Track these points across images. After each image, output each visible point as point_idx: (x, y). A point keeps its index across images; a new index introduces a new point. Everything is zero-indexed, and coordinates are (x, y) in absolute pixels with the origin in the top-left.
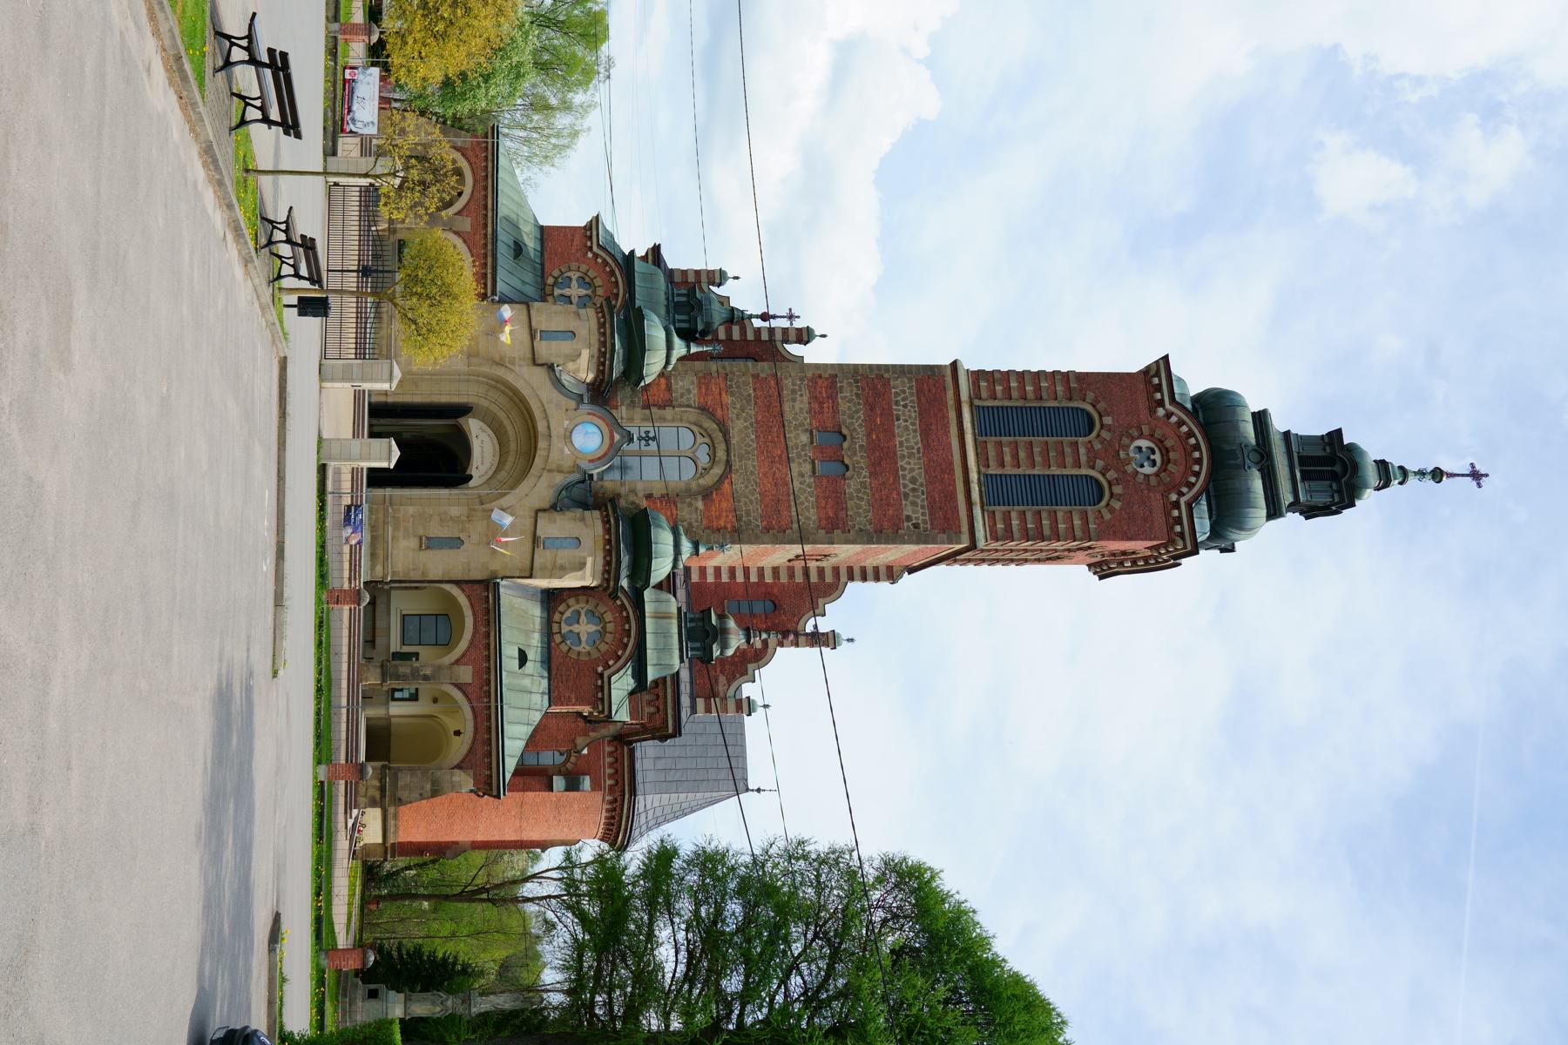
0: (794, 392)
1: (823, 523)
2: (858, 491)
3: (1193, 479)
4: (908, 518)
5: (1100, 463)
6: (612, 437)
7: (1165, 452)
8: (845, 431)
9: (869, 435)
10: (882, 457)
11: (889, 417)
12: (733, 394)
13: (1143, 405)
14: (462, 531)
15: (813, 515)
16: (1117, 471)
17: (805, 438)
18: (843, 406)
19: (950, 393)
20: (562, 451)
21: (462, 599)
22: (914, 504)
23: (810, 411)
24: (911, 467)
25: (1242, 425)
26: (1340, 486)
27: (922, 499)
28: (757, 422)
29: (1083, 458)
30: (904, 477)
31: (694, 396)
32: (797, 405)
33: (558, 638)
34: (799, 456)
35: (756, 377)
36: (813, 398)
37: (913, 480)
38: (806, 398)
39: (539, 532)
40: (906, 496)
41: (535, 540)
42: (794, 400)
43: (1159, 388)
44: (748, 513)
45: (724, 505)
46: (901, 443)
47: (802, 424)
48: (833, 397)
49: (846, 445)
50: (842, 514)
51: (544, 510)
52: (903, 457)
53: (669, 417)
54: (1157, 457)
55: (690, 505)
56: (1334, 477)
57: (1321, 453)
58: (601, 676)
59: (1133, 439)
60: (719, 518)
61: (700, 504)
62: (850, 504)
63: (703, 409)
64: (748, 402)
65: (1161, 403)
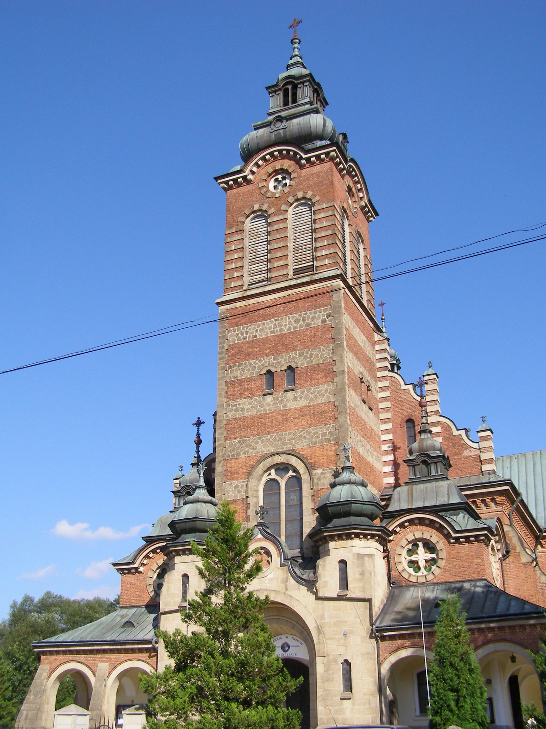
0: (237, 410)
1: (328, 379)
2: (305, 357)
3: (292, 153)
4: (323, 321)
5: (284, 207)
6: (260, 540)
7: (276, 172)
8: (264, 371)
9: (267, 355)
10: (281, 344)
11: (255, 342)
12: (238, 454)
13: (246, 188)
14: (336, 661)
15: (323, 388)
16: (288, 197)
17: (269, 398)
18: (247, 374)
19: (238, 304)
20: (272, 579)
21: (393, 658)
22: (313, 319)
23: (250, 397)
24: (287, 323)
25: (262, 136)
26: (300, 83)
27: (310, 314)
28: (258, 434)
29: (281, 217)
30: (295, 328)
31: (240, 483)
32: (246, 407)
33: (430, 577)
34: (282, 401)
35: (226, 438)
36: (241, 396)
37: (297, 321)
38: (241, 401)
39: (335, 595)
40: (308, 325)
41: (340, 598)
42: (243, 409)
43: (235, 181)
44: (324, 434)
45: (318, 453)
46: (271, 332)
47: (260, 402)
48: (241, 382)
49: (273, 370)
50: (322, 367)
51: (316, 593)
52: (281, 330)
53: (255, 500)
54: (280, 177)
55: (319, 479)
56: (295, 87)
57: (281, 95)
58: (457, 539)
59: (268, 191)
60: (328, 456)
61: (319, 471)
62: (315, 362)
63: (249, 474)
64: (244, 442)
65: (245, 178)
